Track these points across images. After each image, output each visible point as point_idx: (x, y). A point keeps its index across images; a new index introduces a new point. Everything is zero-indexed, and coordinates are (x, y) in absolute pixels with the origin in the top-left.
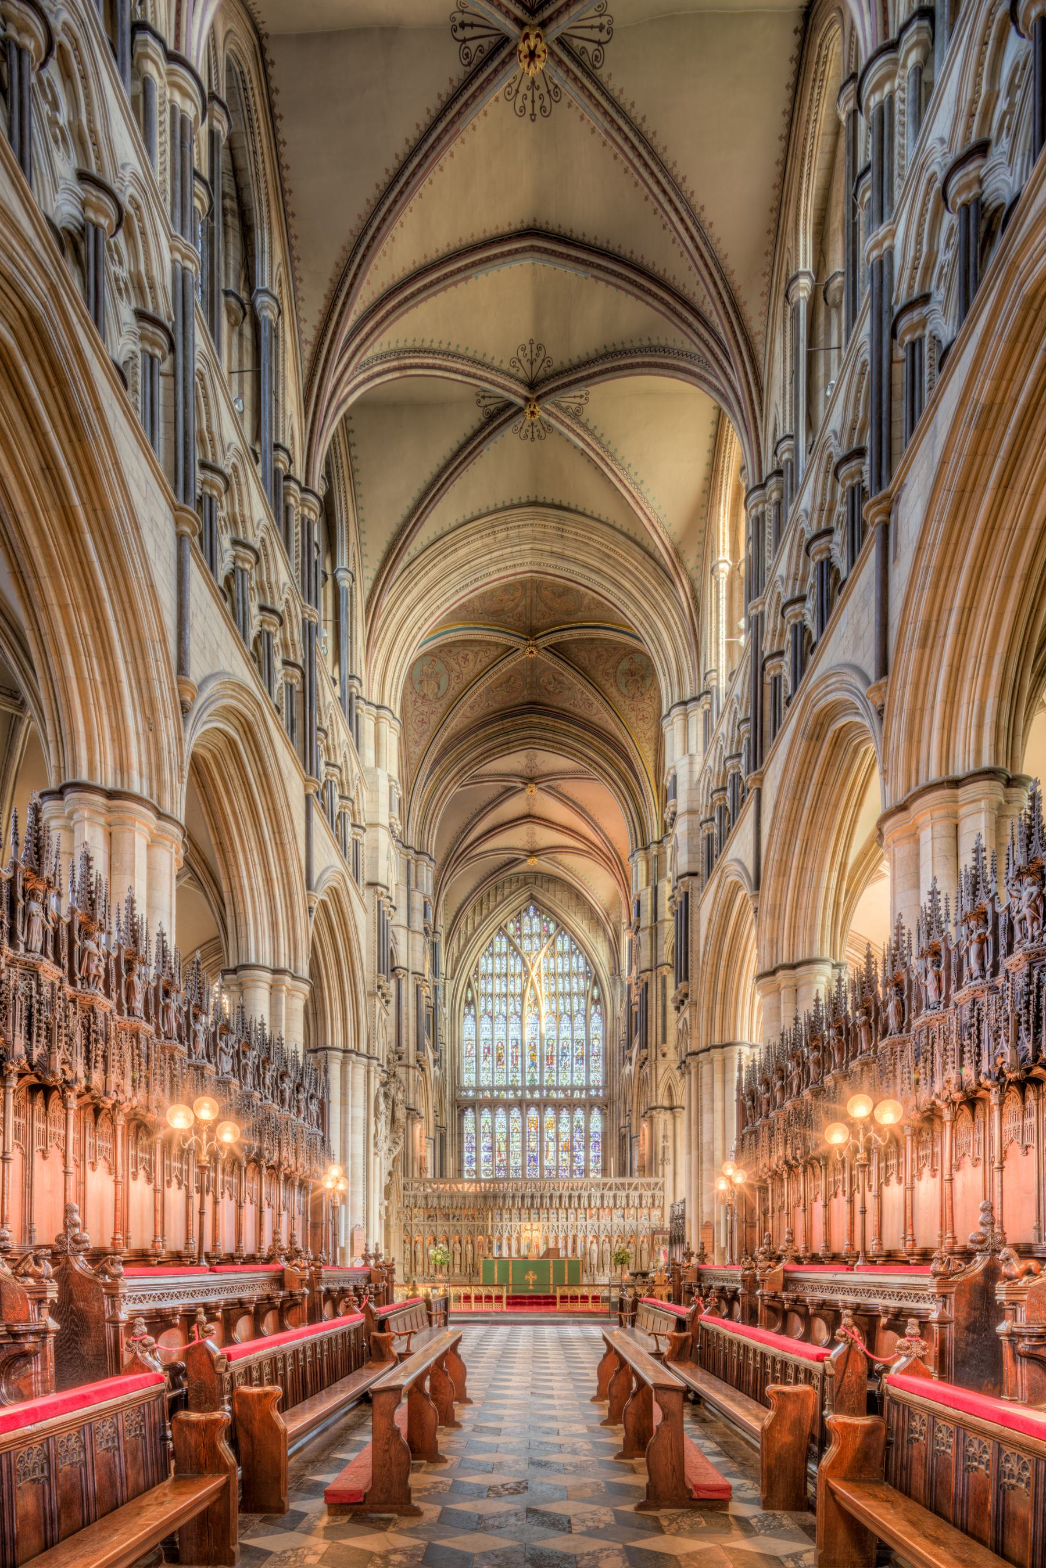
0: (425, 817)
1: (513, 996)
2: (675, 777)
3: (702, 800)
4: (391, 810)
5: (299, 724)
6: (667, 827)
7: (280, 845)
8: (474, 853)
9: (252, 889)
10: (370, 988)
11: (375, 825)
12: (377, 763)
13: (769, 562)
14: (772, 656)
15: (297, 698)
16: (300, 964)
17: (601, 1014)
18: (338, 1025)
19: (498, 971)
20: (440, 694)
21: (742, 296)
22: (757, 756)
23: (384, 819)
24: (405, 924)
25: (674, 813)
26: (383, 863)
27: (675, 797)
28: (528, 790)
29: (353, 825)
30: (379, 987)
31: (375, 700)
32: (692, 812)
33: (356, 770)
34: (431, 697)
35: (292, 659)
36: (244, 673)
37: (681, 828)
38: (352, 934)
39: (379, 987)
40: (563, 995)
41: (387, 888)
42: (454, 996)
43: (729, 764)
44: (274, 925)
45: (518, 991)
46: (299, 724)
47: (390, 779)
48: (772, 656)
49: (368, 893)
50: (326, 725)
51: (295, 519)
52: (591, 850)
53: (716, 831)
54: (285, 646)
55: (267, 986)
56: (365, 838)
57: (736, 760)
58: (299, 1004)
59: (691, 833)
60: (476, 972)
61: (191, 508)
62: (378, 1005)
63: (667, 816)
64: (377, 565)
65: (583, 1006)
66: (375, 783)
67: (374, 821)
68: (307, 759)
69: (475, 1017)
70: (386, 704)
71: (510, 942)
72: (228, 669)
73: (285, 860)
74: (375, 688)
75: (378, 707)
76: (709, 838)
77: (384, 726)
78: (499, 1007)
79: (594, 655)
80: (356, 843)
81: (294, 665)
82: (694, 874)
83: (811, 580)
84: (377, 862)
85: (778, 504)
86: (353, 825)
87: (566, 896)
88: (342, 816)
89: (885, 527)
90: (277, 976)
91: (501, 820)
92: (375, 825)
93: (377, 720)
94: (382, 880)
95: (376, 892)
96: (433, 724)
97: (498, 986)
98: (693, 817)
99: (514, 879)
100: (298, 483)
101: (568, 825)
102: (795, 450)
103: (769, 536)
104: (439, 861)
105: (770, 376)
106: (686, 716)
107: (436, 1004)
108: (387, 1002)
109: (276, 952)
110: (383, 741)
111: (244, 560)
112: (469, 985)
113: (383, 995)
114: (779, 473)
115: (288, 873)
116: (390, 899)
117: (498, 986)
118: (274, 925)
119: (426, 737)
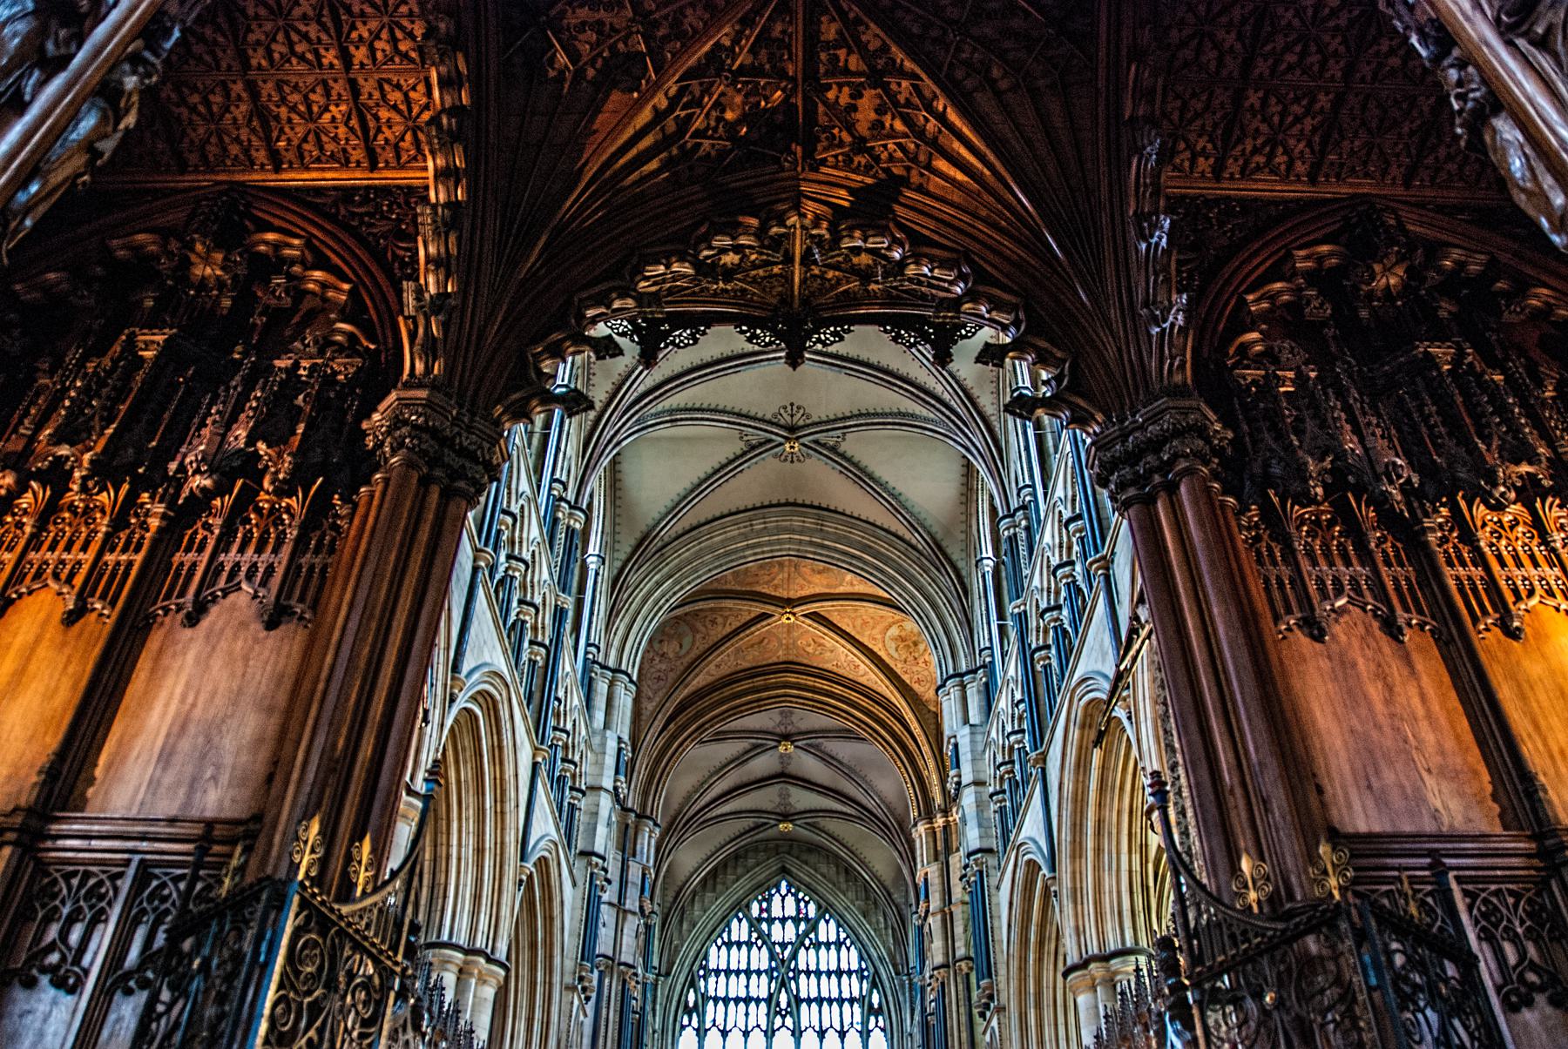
0: (651, 776)
1: (758, 1001)
2: (956, 746)
3: (988, 772)
4: (617, 772)
5: (537, 696)
6: (952, 799)
7: (501, 815)
8: (709, 816)
9: (459, 859)
10: (568, 979)
11: (597, 789)
12: (607, 726)
13: (1026, 572)
14: (1039, 649)
15: (538, 673)
16: (499, 945)
17: (883, 1030)
18: (522, 1026)
19: (734, 966)
20: (683, 652)
21: (975, 392)
22: (1040, 734)
23: (608, 783)
24: (615, 901)
25: (959, 783)
26: (601, 830)
27: (958, 766)
28: (781, 749)
29: (572, 789)
30: (581, 979)
31: (611, 663)
32: (978, 783)
33: (584, 732)
34: (671, 655)
35: (540, 639)
36: (502, 665)
37: (968, 798)
38: (557, 911)
39: (581, 979)
40: (830, 1001)
41: (604, 859)
42: (669, 999)
43: (1012, 738)
44: (477, 897)
45: (764, 994)
46: (537, 696)
47: (620, 740)
48: (1039, 649)
49: (580, 864)
50: (561, 694)
51: (561, 527)
52: (865, 815)
53: (1008, 804)
54: (535, 628)
55: (456, 969)
56: (583, 804)
57: (1019, 736)
58: (489, 992)
59: (980, 806)
60: (701, 967)
61: (489, 550)
62: (576, 1002)
63: (951, 787)
64: (629, 550)
65: (858, 1018)
66: (603, 744)
67: (596, 784)
68: (538, 727)
69: (698, 1030)
70: (623, 667)
71: (754, 924)
72: (488, 660)
73: (503, 829)
74: (613, 653)
75: (614, 671)
76: (1002, 811)
77: (620, 690)
78: (736, 1014)
79: (859, 622)
80: (572, 807)
81: (541, 645)
82: (989, 851)
83: (1063, 594)
84: (595, 829)
85: (1028, 529)
86: (572, 789)
87: (831, 870)
88: (561, 779)
89: (1107, 578)
90: (470, 958)
91: (745, 779)
92: (597, 789)
93: (611, 685)
94: (599, 848)
95: (590, 864)
96: (670, 680)
97: (737, 987)
98: (980, 789)
99: (762, 847)
100: (568, 503)
101: (832, 785)
102: (1034, 494)
103: (1023, 552)
104: (664, 825)
105: (1007, 442)
106: (963, 687)
107: (643, 1008)
108: (588, 999)
109: (473, 930)
110: (616, 703)
111: (515, 570)
112: (693, 985)
113: (584, 989)
114: (1024, 507)
115: (502, 843)
116: (606, 870)
117: (737, 987)
118: (477, 897)
119: (661, 694)
